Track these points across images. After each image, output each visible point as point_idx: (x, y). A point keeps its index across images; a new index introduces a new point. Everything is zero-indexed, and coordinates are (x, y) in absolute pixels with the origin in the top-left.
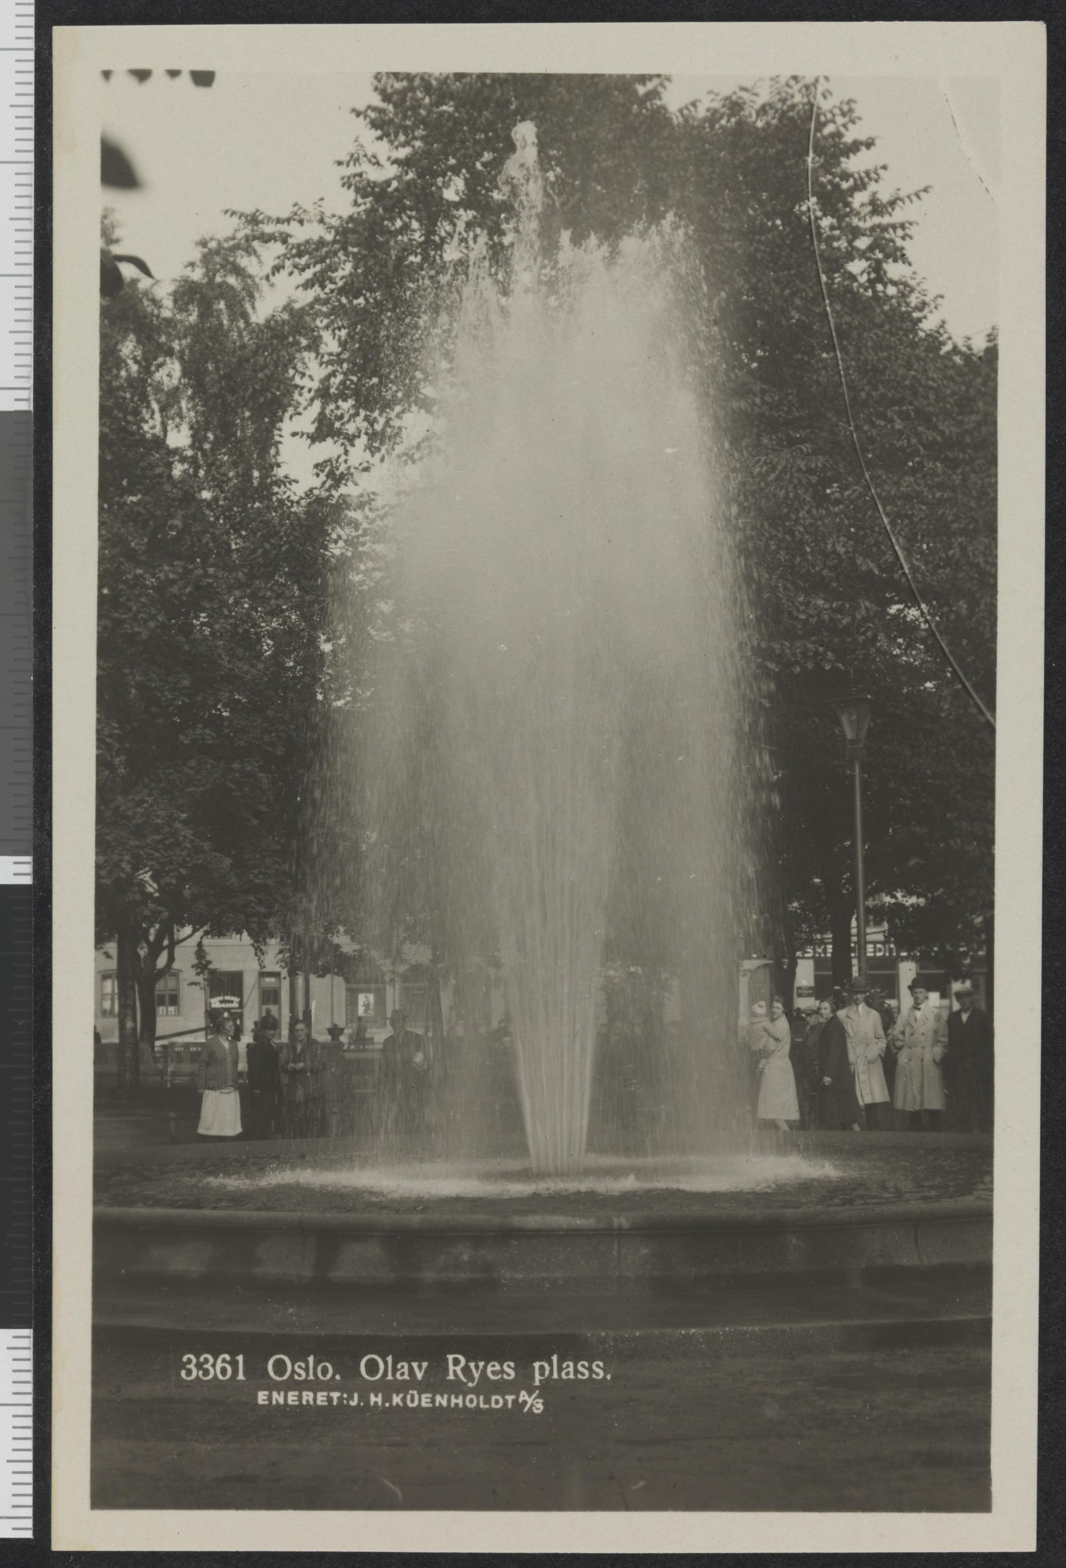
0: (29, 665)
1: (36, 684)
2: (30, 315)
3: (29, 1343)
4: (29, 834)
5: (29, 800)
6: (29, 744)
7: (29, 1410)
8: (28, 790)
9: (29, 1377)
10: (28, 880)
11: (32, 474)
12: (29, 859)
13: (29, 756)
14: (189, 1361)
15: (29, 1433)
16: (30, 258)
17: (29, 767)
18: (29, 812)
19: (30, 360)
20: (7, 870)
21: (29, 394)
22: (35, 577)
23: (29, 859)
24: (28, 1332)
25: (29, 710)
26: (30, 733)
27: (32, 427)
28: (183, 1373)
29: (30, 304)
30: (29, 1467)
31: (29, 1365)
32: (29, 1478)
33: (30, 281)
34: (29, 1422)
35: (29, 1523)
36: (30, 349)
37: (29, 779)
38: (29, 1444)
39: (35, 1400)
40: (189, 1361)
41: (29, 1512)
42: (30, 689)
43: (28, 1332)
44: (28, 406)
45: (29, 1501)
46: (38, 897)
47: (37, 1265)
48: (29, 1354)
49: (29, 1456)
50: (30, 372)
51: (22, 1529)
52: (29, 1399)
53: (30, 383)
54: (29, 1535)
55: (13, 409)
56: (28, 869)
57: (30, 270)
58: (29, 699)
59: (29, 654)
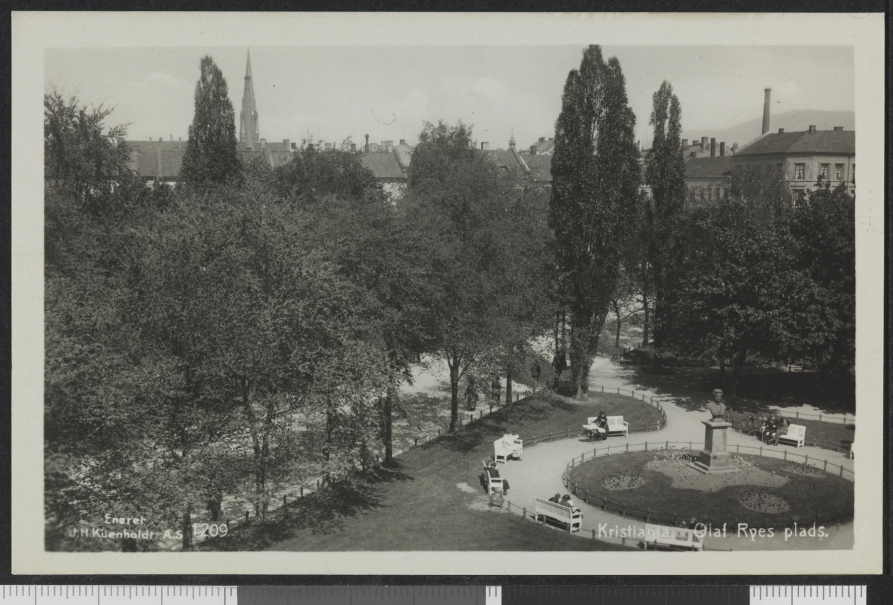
0: (380, 588)
1: (390, 584)
2: (184, 588)
3: (757, 588)
4: (474, 588)
5: (455, 588)
6: (424, 587)
7: (795, 587)
8: (449, 588)
9: (776, 587)
10: (499, 588)
12: (487, 588)
13: (430, 588)
15: (808, 587)
16: (152, 587)
17: (436, 588)
18: (461, 588)
19: (209, 588)
20: (494, 600)
21: (228, 588)
22: (330, 584)
23: (487, 588)
24: (751, 588)
25: (404, 588)
26: (417, 588)
27: (246, 587)
29: (178, 587)
30: (827, 587)
31: (770, 587)
32: (833, 587)
33: (165, 587)
34: (802, 587)
35: (858, 587)
36: (203, 588)
37: (443, 588)
38: (814, 587)
39: (790, 584)
41: (852, 587)
42: (393, 587)
43: (751, 588)
44: (235, 589)
45: (846, 587)
46: (508, 583)
48: (764, 588)
49: (820, 587)
50: (215, 588)
51: (861, 591)
52: (789, 587)
53: (222, 587)
54: (865, 588)
56: (493, 588)
57: (159, 587)
58: (398, 588)
59: (373, 588)
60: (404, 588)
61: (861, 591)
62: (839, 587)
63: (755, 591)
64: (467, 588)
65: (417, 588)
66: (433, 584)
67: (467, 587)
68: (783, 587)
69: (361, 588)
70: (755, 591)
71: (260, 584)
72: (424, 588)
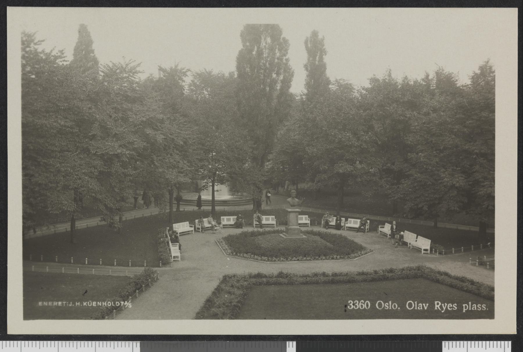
0: (224, 342)
1: (230, 340)
2: (108, 342)
3: (447, 342)
4: (279, 342)
5: (268, 342)
6: (250, 342)
7: (469, 342)
8: (265, 343)
9: (458, 342)
10: (295, 343)
11: (161, 342)
12: (287, 342)
13: (254, 342)
14: (351, 303)
15: (477, 342)
16: (90, 342)
17: (257, 342)
18: (272, 342)
19: (123, 342)
21: (135, 343)
22: (195, 340)
23: (287, 342)
24: (443, 342)
26: (246, 342)
27: (145, 342)
28: (349, 307)
29: (105, 342)
30: (488, 342)
31: (454, 342)
32: (491, 342)
33: (97, 342)
34: (473, 342)
35: (506, 342)
36: (120, 342)
37: (261, 342)
38: (480, 342)
40: (351, 303)
41: (503, 342)
42: (232, 342)
43: (443, 342)
44: (138, 343)
45: (499, 342)
47: (421, 340)
48: (451, 342)
49: (484, 342)
50: (127, 342)
51: (508, 345)
52: (465, 342)
53: (131, 342)
54: (510, 342)
55: (139, 348)
56: (291, 343)
57: (94, 342)
58: (235, 343)
59: (220, 343)
60: (239, 343)
61: (508, 345)
62: (495, 342)
63: (445, 344)
64: (276, 343)
65: (246, 343)
66: (255, 340)
67: (275, 342)
68: (462, 342)
69: (213, 343)
70: (445, 344)
71: (153, 340)
72: (250, 342)
